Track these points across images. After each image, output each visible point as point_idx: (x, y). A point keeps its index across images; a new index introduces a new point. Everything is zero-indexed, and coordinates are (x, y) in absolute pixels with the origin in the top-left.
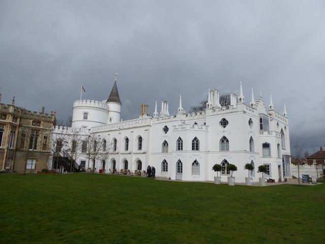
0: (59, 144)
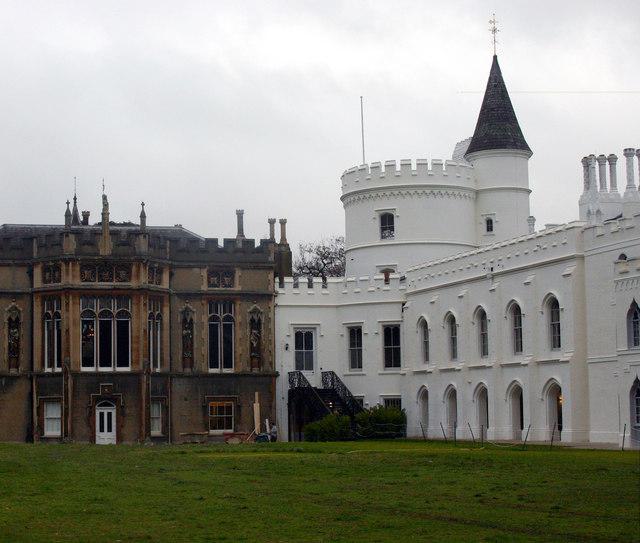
0: (304, 340)
